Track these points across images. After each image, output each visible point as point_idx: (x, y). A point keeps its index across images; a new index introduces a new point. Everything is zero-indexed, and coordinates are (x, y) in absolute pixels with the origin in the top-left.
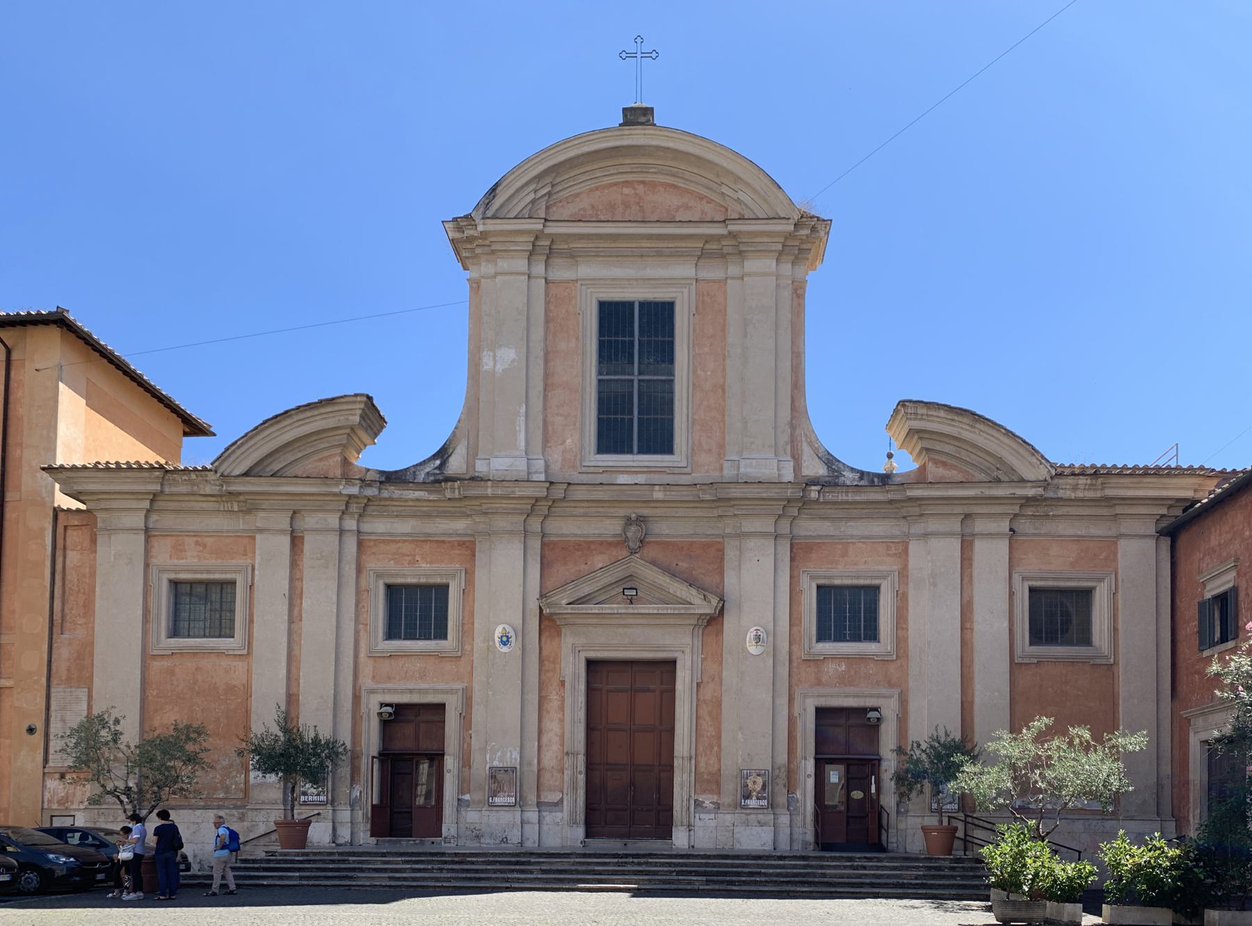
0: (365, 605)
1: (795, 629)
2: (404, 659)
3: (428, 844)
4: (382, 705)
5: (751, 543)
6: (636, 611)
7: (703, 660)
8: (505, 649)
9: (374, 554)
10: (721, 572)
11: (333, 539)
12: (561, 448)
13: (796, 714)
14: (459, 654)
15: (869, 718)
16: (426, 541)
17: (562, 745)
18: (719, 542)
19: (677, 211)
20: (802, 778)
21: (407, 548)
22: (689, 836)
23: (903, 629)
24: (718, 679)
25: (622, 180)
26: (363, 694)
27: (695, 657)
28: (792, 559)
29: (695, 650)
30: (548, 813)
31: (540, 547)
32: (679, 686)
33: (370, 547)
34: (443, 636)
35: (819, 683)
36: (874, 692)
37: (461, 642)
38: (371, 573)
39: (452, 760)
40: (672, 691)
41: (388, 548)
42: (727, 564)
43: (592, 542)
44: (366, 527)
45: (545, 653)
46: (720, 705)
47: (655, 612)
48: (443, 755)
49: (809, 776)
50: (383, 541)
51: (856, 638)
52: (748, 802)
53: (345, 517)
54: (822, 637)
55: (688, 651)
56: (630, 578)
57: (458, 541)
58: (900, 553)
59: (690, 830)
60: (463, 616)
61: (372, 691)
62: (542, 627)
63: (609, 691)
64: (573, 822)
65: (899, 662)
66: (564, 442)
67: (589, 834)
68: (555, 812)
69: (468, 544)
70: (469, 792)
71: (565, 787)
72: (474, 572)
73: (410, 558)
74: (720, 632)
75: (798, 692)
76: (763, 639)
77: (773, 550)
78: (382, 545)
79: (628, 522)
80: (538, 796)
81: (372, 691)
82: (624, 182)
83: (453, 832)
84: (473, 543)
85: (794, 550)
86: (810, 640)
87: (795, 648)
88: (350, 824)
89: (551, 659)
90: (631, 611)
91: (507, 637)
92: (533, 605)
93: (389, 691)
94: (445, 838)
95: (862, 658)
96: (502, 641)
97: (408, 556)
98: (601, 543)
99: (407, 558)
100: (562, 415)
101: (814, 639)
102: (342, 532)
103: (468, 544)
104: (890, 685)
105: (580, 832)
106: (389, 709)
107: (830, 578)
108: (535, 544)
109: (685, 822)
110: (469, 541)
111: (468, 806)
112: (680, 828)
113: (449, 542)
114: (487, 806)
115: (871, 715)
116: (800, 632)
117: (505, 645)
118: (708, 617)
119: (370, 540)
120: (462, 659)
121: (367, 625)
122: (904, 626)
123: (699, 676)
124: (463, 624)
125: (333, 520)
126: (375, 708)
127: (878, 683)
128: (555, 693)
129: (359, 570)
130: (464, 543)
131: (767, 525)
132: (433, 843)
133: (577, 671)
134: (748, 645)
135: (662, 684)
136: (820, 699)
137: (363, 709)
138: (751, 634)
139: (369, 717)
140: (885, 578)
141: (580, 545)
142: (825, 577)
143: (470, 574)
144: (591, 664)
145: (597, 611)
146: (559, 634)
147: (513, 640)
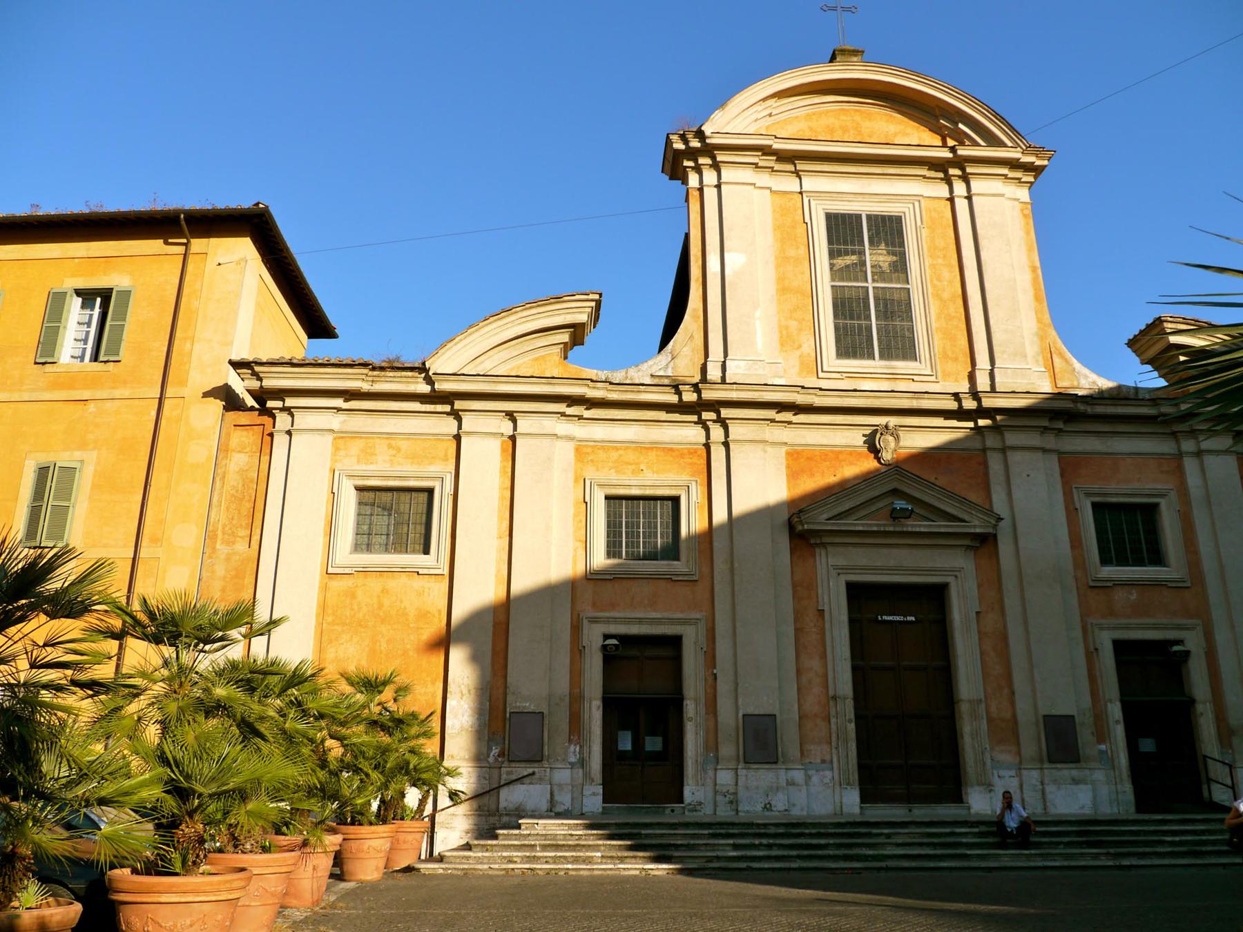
3: (668, 811)
4: (606, 637)
12: (798, 353)
16: (652, 448)
17: (827, 687)
19: (895, 137)
21: (631, 456)
26: (585, 622)
30: (814, 772)
33: (588, 453)
49: (1117, 722)
54: (1105, 561)
57: (688, 449)
61: (594, 620)
66: (800, 347)
68: (823, 770)
73: (634, 466)
78: (601, 451)
93: (615, 620)
98: (851, 453)
99: (630, 467)
100: (795, 320)
106: (614, 642)
113: (678, 450)
115: (1176, 648)
140: (1162, 496)
141: (827, 455)
142: (1099, 494)
145: (861, 528)
146: (814, 556)
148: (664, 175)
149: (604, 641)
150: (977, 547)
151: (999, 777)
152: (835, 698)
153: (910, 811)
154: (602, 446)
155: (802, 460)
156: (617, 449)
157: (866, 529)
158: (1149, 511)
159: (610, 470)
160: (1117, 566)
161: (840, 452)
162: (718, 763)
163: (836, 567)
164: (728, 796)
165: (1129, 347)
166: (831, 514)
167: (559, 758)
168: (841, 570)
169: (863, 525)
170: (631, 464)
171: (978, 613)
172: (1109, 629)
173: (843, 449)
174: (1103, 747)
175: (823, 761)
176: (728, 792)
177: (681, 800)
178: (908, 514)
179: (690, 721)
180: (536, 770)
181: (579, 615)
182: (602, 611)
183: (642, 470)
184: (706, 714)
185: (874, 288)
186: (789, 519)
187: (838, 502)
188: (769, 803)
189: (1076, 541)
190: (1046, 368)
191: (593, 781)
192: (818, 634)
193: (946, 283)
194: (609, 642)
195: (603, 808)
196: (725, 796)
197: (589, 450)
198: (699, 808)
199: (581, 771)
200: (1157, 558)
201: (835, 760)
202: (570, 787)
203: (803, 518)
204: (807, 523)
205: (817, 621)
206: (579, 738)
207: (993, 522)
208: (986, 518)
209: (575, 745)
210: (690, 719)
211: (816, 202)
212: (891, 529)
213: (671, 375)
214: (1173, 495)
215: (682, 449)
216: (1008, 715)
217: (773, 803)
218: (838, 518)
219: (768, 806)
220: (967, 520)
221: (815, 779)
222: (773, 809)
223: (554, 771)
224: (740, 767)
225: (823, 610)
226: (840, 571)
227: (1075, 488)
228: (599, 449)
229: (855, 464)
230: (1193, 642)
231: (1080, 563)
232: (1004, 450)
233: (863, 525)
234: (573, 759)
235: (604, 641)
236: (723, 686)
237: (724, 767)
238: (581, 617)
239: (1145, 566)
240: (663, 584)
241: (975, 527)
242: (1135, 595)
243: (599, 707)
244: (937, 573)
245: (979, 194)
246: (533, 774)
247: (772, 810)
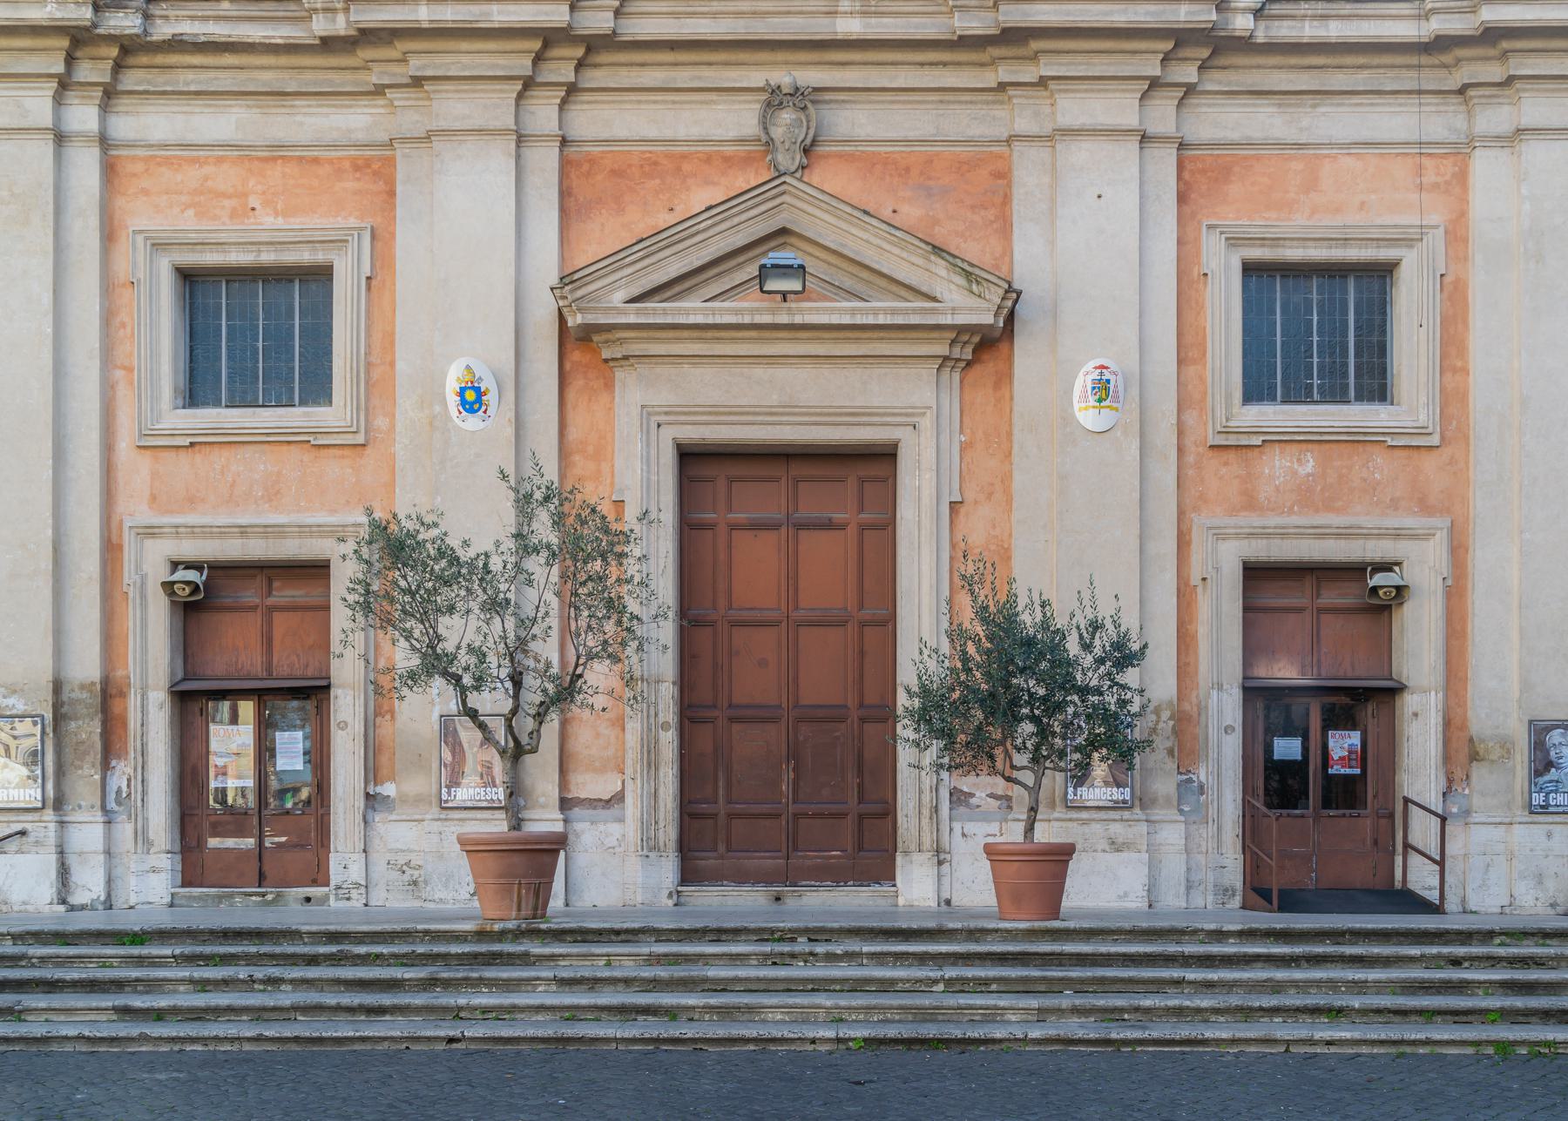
0: (126, 319)
1: (1191, 370)
2: (226, 453)
4: (175, 565)
5: (1079, 153)
6: (798, 319)
7: (964, 448)
8: (473, 423)
9: (145, 192)
10: (1004, 227)
11: (46, 147)
13: (1195, 579)
14: (360, 439)
15: (1374, 590)
16: (274, 159)
18: (1000, 156)
20: (1213, 734)
22: (939, 876)
23: (1455, 370)
24: (1001, 490)
27: (945, 438)
28: (1182, 198)
29: (945, 422)
31: (556, 165)
32: (906, 512)
33: (135, 175)
34: (317, 388)
35: (1250, 503)
36: (1392, 522)
37: (366, 408)
38: (140, 239)
39: (349, 699)
40: (888, 526)
41: (179, 177)
42: (1019, 208)
43: (684, 156)
44: (124, 126)
45: (573, 434)
46: (1009, 558)
47: (846, 320)
48: (328, 687)
50: (167, 162)
51: (1335, 394)
52: (1083, 791)
53: (72, 97)
54: (1256, 390)
55: (926, 423)
56: (780, 240)
57: (353, 160)
58: (1446, 182)
59: (940, 863)
60: (368, 346)
61: (150, 532)
62: (568, 366)
63: (734, 527)
64: (650, 846)
65: (1446, 452)
67: (689, 875)
68: (606, 822)
69: (375, 166)
70: (392, 778)
71: (629, 762)
72: (393, 235)
73: (234, 202)
74: (1005, 378)
75: (1200, 522)
76: (1116, 392)
77: (1135, 170)
78: (163, 169)
79: (775, 99)
80: (563, 784)
81: (150, 532)
83: (356, 873)
84: (390, 162)
85: (1186, 175)
86: (1229, 396)
87: (1191, 418)
88: (102, 857)
89: (590, 449)
90: (783, 319)
91: (477, 390)
92: (543, 310)
93: (193, 531)
94: (338, 888)
95: (1358, 440)
96: (463, 402)
97: (230, 197)
98: (708, 159)
99: (227, 203)
101: (1238, 394)
102: (60, 138)
103: (375, 166)
104: (1426, 508)
105: (667, 870)
107: (1276, 241)
108: (546, 159)
109: (927, 841)
110: (380, 159)
111: (391, 810)
112: (916, 857)
113: (331, 161)
114: (435, 809)
115: (1378, 579)
116: (1202, 379)
117: (472, 411)
118: (976, 339)
119: (134, 159)
120: (369, 450)
121: (130, 370)
122: (1459, 364)
123: (956, 486)
124: (369, 365)
125: (38, 104)
126: (158, 572)
127: (1394, 505)
129: (109, 235)
130: (368, 162)
131: (1121, 109)
132: (308, 900)
133: (654, 478)
134: (1076, 406)
135: (861, 509)
136: (1253, 542)
137: (129, 576)
138: (1084, 380)
139: (143, 596)
140: (1409, 242)
141: (656, 163)
143: (381, 239)
144: (690, 458)
146: (609, 385)
147: (491, 398)
151: (964, 835)
154: (167, 158)
155: (599, 177)
164: (409, 872)
167: (83, 803)
170: (224, 195)
173: (693, 149)
183: (253, 209)
194: (182, 574)
196: (404, 872)
215: (340, 159)
225: (623, 501)
227: (1210, 227)
228: (159, 164)
229: (714, 184)
237: (404, 817)
242: (1312, 463)
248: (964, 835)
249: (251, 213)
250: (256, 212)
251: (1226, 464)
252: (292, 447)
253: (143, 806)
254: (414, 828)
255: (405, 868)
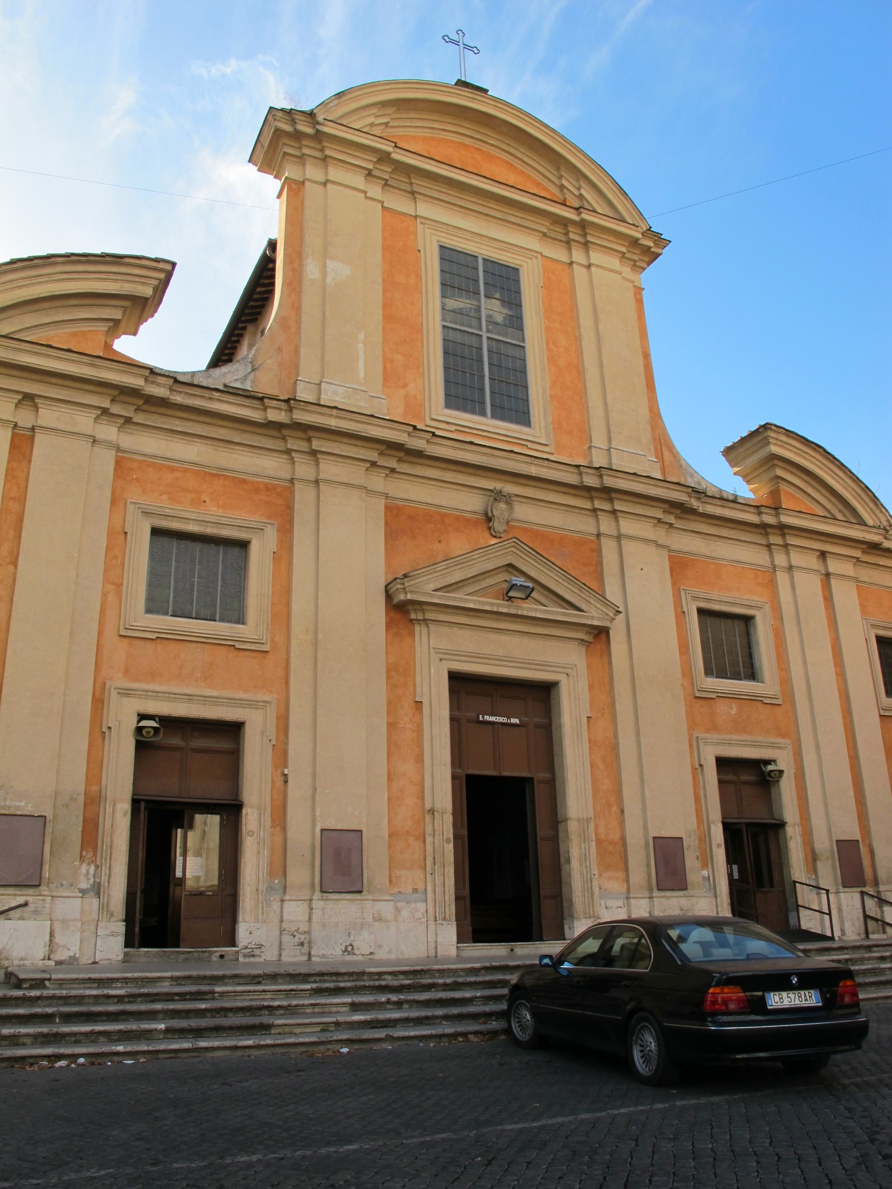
3: (215, 958)
4: (142, 717)
12: (403, 392)
17: (422, 798)
25: (459, 140)
26: (114, 693)
35: (714, 728)
54: (708, 672)
57: (266, 485)
61: (126, 693)
66: (405, 386)
68: (415, 902)
69: (279, 490)
82: (460, 143)
98: (458, 518)
104: (783, 736)
113: (252, 483)
119: (132, 460)
128: (406, 719)
130: (274, 488)
141: (431, 516)
145: (471, 606)
146: (412, 634)
148: (251, 165)
149: (138, 723)
150: (590, 643)
151: (606, 907)
152: (432, 811)
153: (512, 950)
154: (153, 463)
156: (173, 470)
157: (477, 607)
158: (747, 620)
159: (161, 495)
160: (717, 677)
161: (446, 515)
162: (285, 892)
163: (438, 651)
164: (298, 936)
165: (723, 455)
166: (439, 586)
167: (65, 883)
168: (444, 655)
169: (474, 602)
170: (190, 492)
171: (588, 717)
172: (712, 743)
174: (705, 873)
175: (415, 891)
176: (297, 930)
177: (232, 941)
178: (528, 594)
179: (251, 836)
180: (30, 899)
181: (104, 684)
182: (138, 681)
183: (205, 502)
184: (272, 827)
185: (488, 338)
186: (386, 587)
187: (446, 571)
188: (351, 945)
189: (684, 648)
190: (656, 458)
191: (112, 915)
192: (414, 731)
193: (562, 350)
194: (144, 723)
195: (126, 954)
196: (294, 936)
197: (135, 465)
198: (257, 952)
199: (95, 901)
200: (752, 674)
201: (429, 888)
202: (79, 924)
203: (406, 585)
204: (411, 592)
205: (414, 716)
206: (95, 855)
207: (612, 615)
208: (604, 609)
209: (89, 864)
210: (251, 834)
211: (431, 231)
212: (505, 610)
213: (249, 389)
214: (767, 608)
215: (258, 482)
216: (616, 836)
217: (355, 944)
218: (444, 590)
219: (349, 948)
220: (584, 609)
221: (405, 913)
222: (355, 951)
223: (57, 901)
224: (315, 897)
225: (421, 702)
226: (442, 656)
227: (683, 589)
228: (148, 466)
230: (784, 761)
231: (687, 672)
232: (619, 538)
233: (474, 602)
234: (84, 885)
235: (138, 722)
236: (296, 792)
237: (294, 898)
238: (107, 686)
239: (741, 680)
240: (223, 651)
241: (593, 618)
243: (125, 814)
244: (549, 668)
245: (598, 266)
246: (26, 904)
247: (354, 954)
248: (606, 907)
249: (203, 504)
250: (207, 504)
251: (702, 706)
252: (221, 648)
253: (109, 886)
254: (301, 906)
255: (295, 933)
